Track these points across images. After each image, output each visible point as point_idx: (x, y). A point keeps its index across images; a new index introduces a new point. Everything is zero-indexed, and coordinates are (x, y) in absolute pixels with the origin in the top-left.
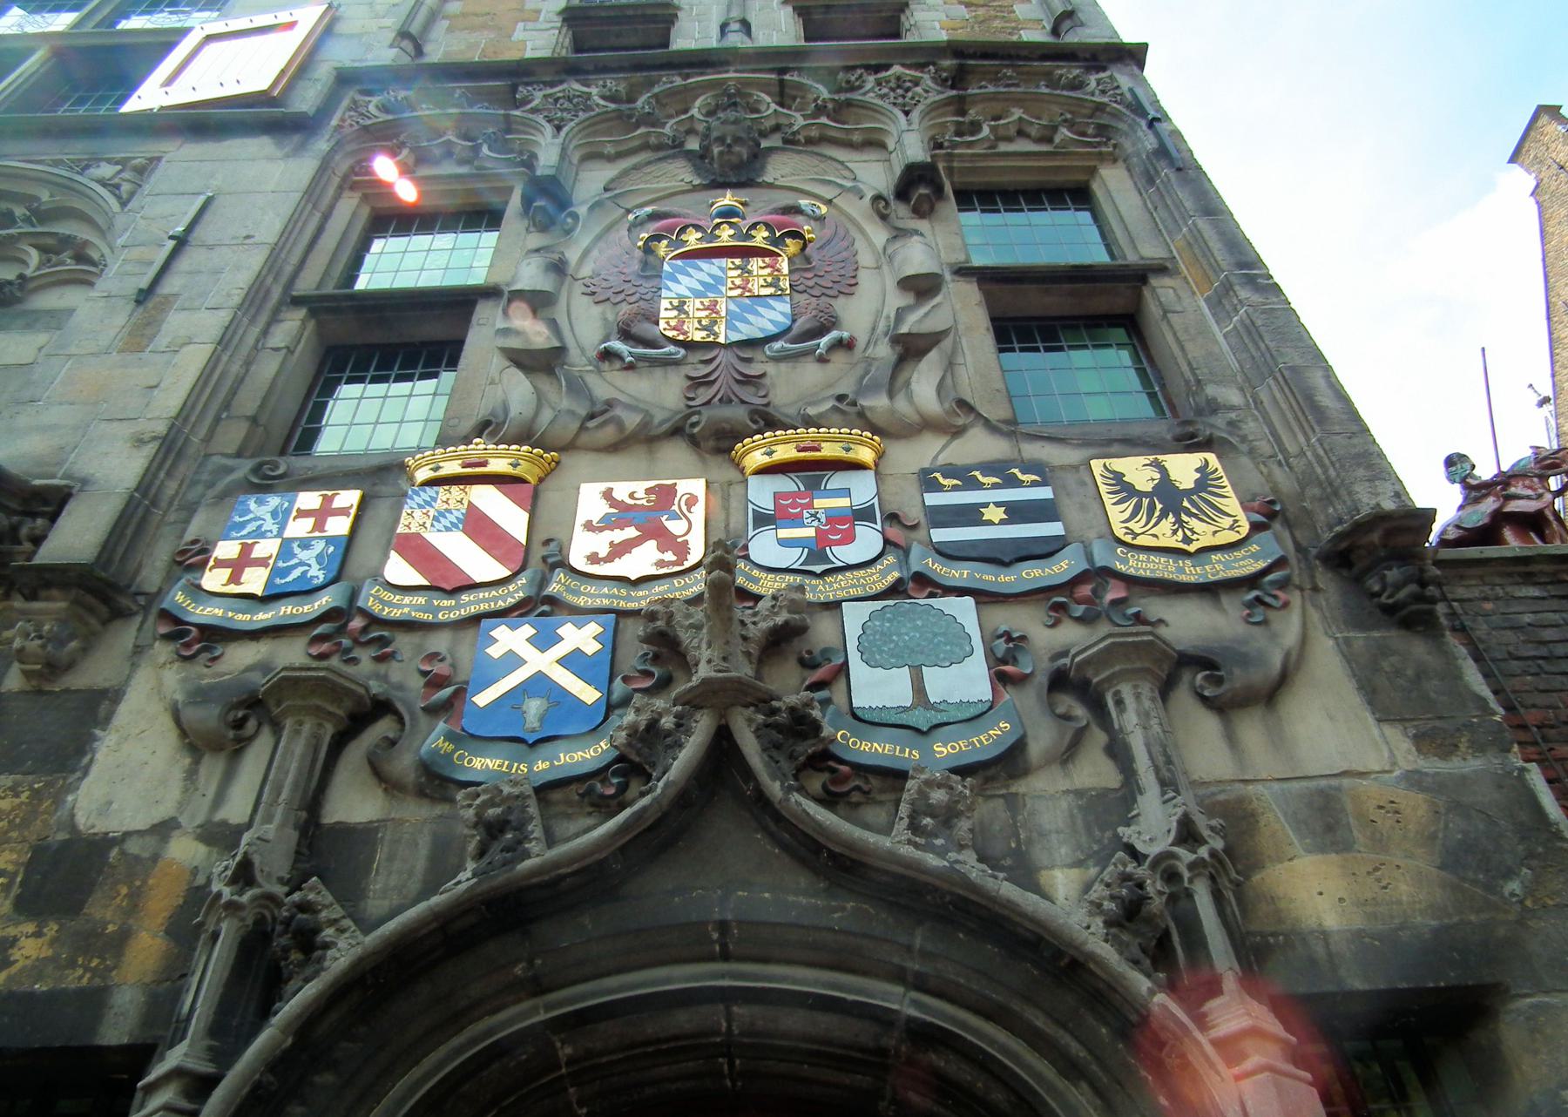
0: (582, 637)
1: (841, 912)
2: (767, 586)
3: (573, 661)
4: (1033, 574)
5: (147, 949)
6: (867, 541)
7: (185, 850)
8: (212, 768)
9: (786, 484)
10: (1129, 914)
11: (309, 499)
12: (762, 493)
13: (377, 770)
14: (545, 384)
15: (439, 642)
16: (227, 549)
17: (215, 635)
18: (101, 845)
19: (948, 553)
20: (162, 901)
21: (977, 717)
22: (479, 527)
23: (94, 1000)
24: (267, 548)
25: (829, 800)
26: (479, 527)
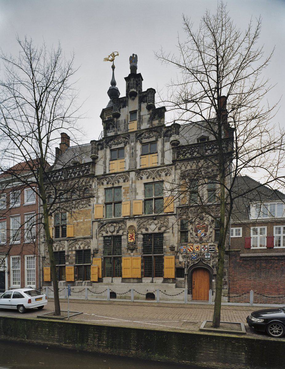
0: (195, 254)
1: (204, 265)
2: (202, 252)
3: (195, 255)
4: (213, 252)
5: (184, 265)
6: (207, 249)
7: (183, 262)
8: (184, 259)
9: (204, 246)
10: (212, 266)
11: (184, 246)
12: (202, 246)
13: (189, 259)
14: (193, 239)
15: (190, 254)
16: (181, 249)
17: (182, 253)
18: (181, 262)
19: (210, 250)
20: (184, 264)
21: (209, 258)
22: (191, 248)
23: (183, 267)
24: (183, 249)
25: (204, 261)
26: (191, 248)
